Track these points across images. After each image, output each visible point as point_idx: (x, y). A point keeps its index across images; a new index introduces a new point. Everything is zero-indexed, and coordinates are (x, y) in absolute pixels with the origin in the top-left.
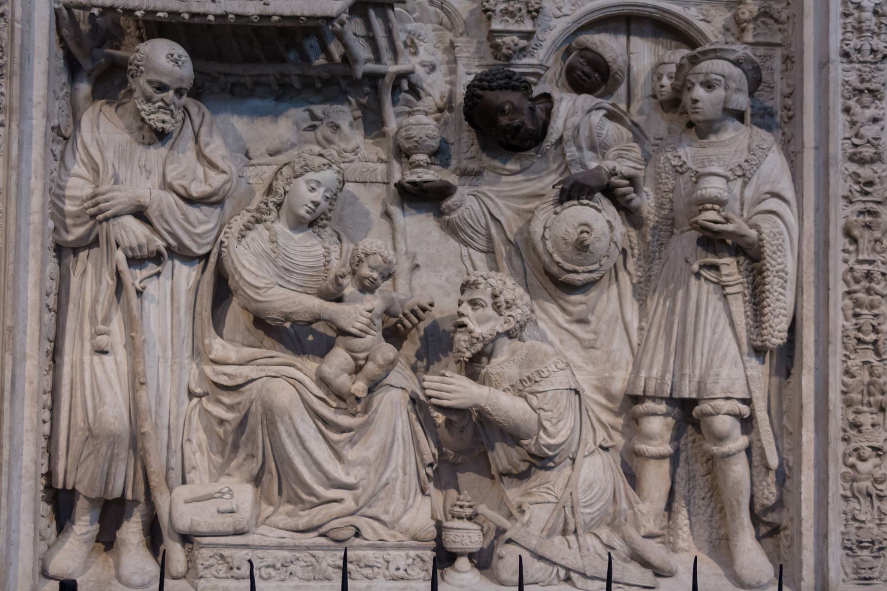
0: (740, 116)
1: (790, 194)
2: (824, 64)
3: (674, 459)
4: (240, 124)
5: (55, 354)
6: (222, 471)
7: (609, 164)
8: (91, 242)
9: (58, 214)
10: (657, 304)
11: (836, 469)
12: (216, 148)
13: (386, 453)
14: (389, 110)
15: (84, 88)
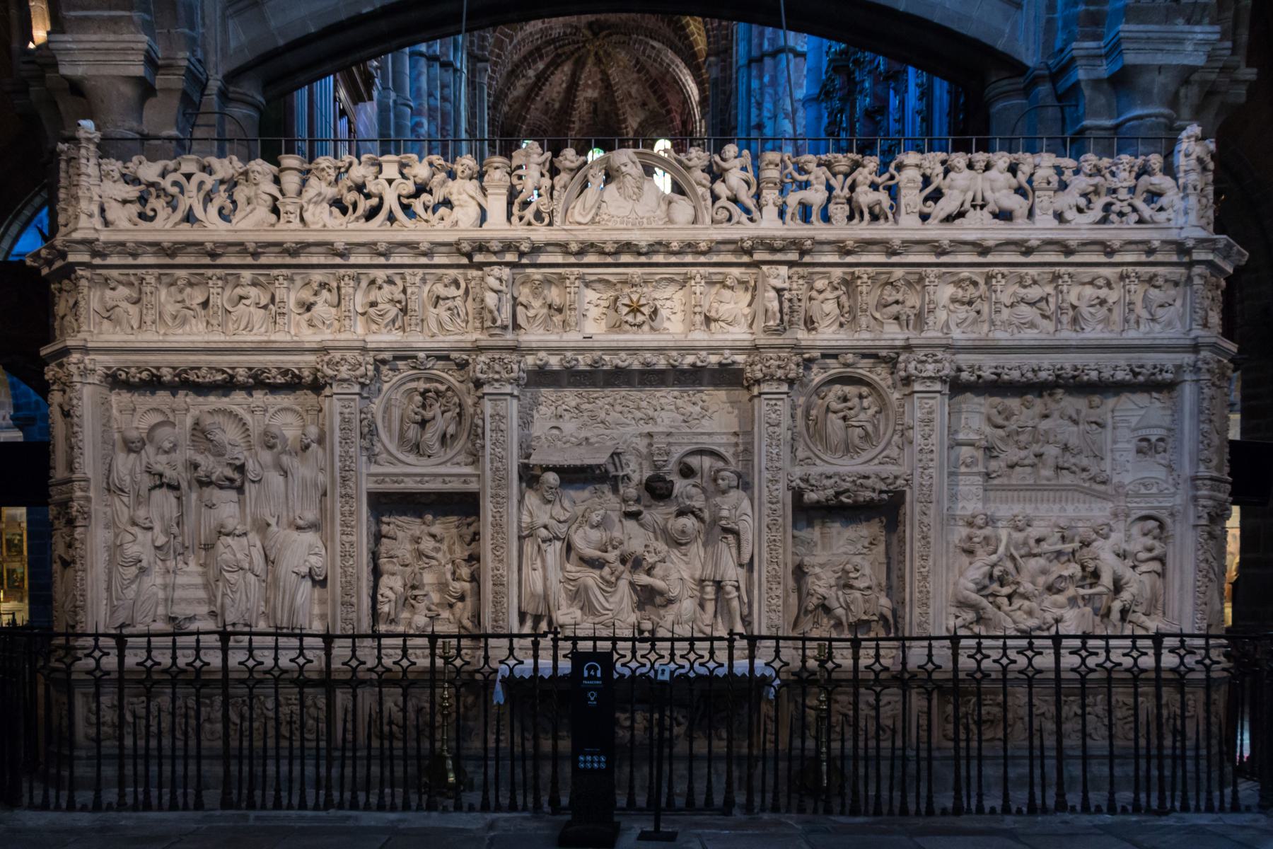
0: (738, 487)
1: (750, 513)
2: (760, 472)
3: (716, 600)
4: (572, 493)
5: (520, 569)
6: (571, 606)
7: (693, 503)
8: (530, 535)
9: (520, 527)
10: (710, 549)
11: (764, 603)
12: (567, 504)
13: (622, 599)
14: (621, 486)
15: (524, 485)
